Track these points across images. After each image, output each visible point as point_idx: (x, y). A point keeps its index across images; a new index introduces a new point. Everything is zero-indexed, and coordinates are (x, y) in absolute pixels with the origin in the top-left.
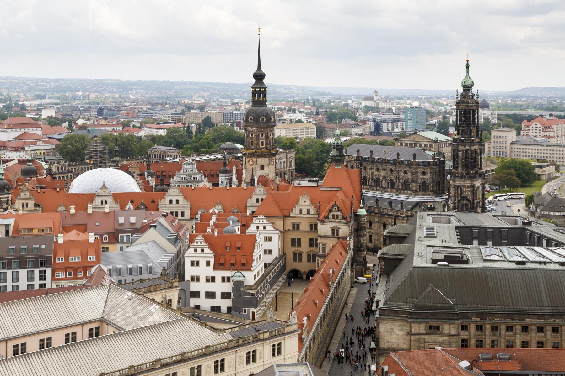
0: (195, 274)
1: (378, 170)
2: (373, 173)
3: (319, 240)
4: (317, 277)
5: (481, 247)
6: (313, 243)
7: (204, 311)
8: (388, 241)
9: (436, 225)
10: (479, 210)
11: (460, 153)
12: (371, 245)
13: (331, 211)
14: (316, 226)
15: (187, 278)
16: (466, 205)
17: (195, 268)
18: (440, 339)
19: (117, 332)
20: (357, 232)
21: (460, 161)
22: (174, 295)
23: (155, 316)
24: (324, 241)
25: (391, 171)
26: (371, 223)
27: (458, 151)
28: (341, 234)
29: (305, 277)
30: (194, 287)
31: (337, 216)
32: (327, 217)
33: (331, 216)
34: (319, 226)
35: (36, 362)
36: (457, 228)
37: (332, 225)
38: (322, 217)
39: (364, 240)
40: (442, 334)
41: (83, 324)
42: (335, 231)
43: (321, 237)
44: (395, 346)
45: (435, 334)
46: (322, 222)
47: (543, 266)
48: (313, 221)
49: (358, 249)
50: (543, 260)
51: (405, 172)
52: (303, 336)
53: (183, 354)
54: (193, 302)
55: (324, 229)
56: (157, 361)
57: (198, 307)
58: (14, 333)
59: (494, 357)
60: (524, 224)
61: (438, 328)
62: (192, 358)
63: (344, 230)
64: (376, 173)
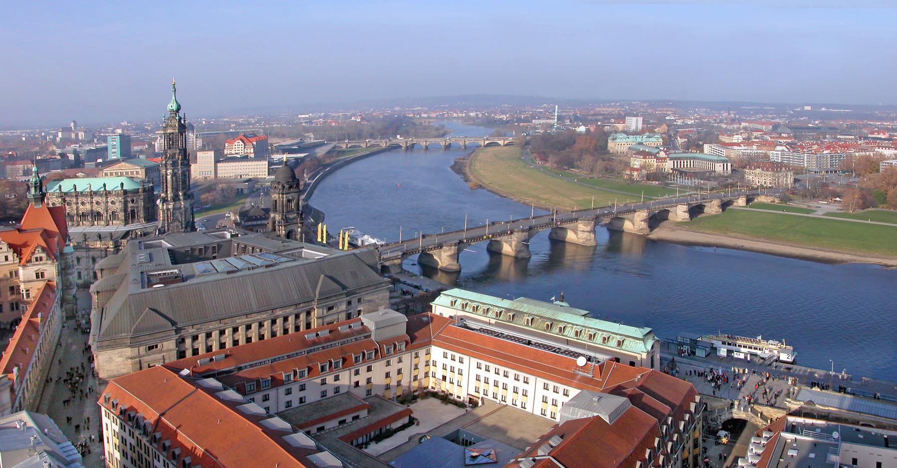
1: (83, 204)
2: (77, 208)
3: (22, 287)
4: (23, 324)
5: (194, 264)
6: (14, 289)
8: (99, 275)
9: (148, 251)
10: (189, 229)
11: (169, 177)
12: (81, 282)
13: (33, 253)
14: (17, 273)
16: (177, 226)
18: (159, 356)
20: (63, 271)
21: (169, 185)
24: (29, 286)
25: (98, 203)
26: (78, 259)
27: (167, 175)
28: (47, 276)
29: (8, 327)
31: (41, 259)
32: (30, 261)
33: (33, 259)
34: (21, 271)
36: (169, 250)
37: (36, 268)
38: (23, 261)
39: (73, 278)
40: (161, 351)
42: (39, 275)
43: (24, 282)
44: (115, 373)
45: (154, 354)
46: (24, 266)
47: (251, 272)
48: (13, 268)
49: (66, 286)
50: (250, 266)
51: (113, 203)
52: (15, 386)
55: (25, 274)
59: (211, 360)
60: (232, 236)
61: (157, 346)
63: (51, 270)
64: (81, 207)
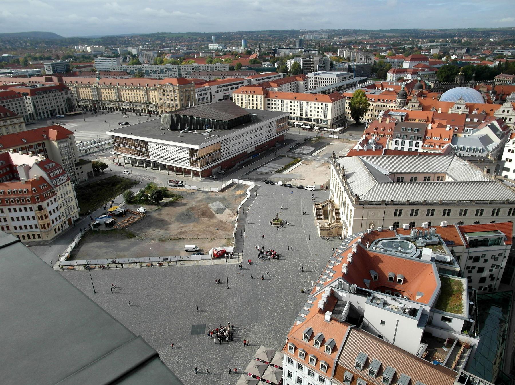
0: (509, 158)
7: (509, 180)
15: (503, 159)
17: (510, 153)
19: (453, 181)
22: (493, 168)
23: (478, 177)
30: (507, 165)
35: (408, 187)
41: (435, 173)
53: (491, 201)
54: (504, 173)
56: (474, 201)
57: (506, 177)
58: (398, 171)
62: (496, 204)
